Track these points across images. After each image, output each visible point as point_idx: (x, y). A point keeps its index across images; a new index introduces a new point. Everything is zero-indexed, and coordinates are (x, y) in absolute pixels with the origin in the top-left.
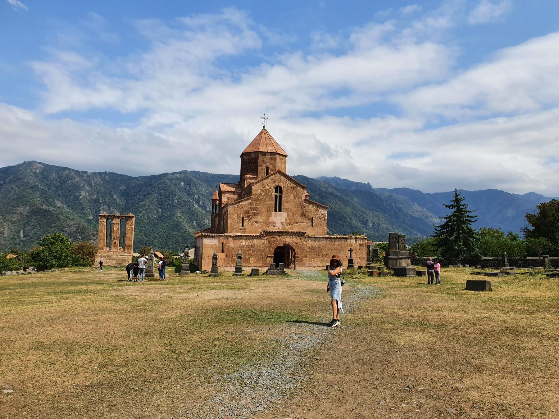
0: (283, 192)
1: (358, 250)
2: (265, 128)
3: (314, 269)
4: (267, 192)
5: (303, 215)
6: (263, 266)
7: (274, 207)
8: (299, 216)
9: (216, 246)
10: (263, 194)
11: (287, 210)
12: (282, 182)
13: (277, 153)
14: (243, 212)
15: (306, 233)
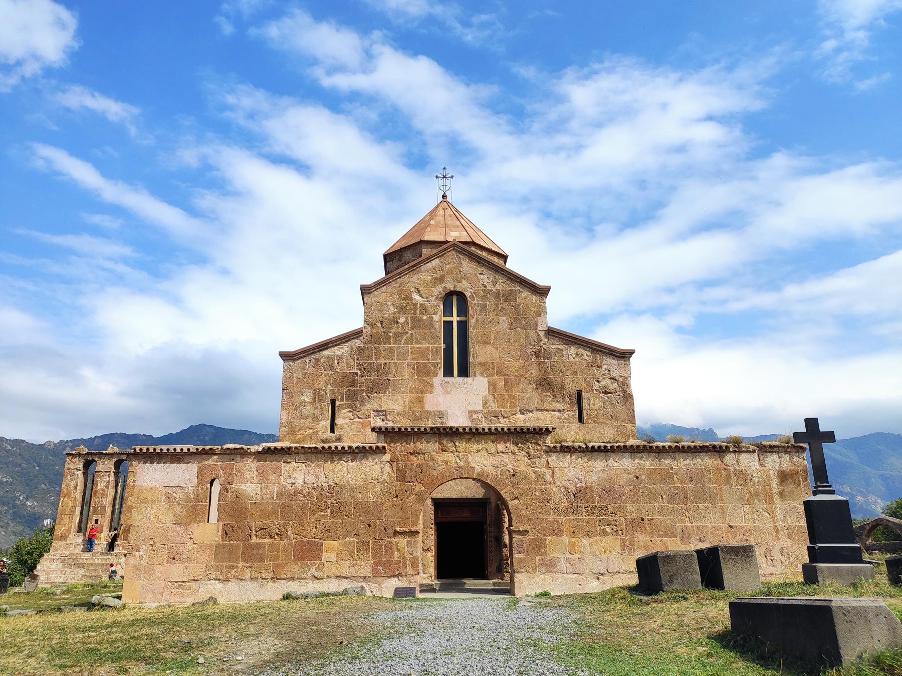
0: (471, 312)
1: (777, 499)
2: (448, 199)
3: (595, 583)
4: (415, 313)
5: (544, 384)
6: (376, 574)
7: (440, 360)
8: (531, 389)
9: (188, 496)
10: (402, 320)
11: (486, 368)
12: (465, 277)
13: (473, 244)
14: (335, 380)
15: (547, 429)
